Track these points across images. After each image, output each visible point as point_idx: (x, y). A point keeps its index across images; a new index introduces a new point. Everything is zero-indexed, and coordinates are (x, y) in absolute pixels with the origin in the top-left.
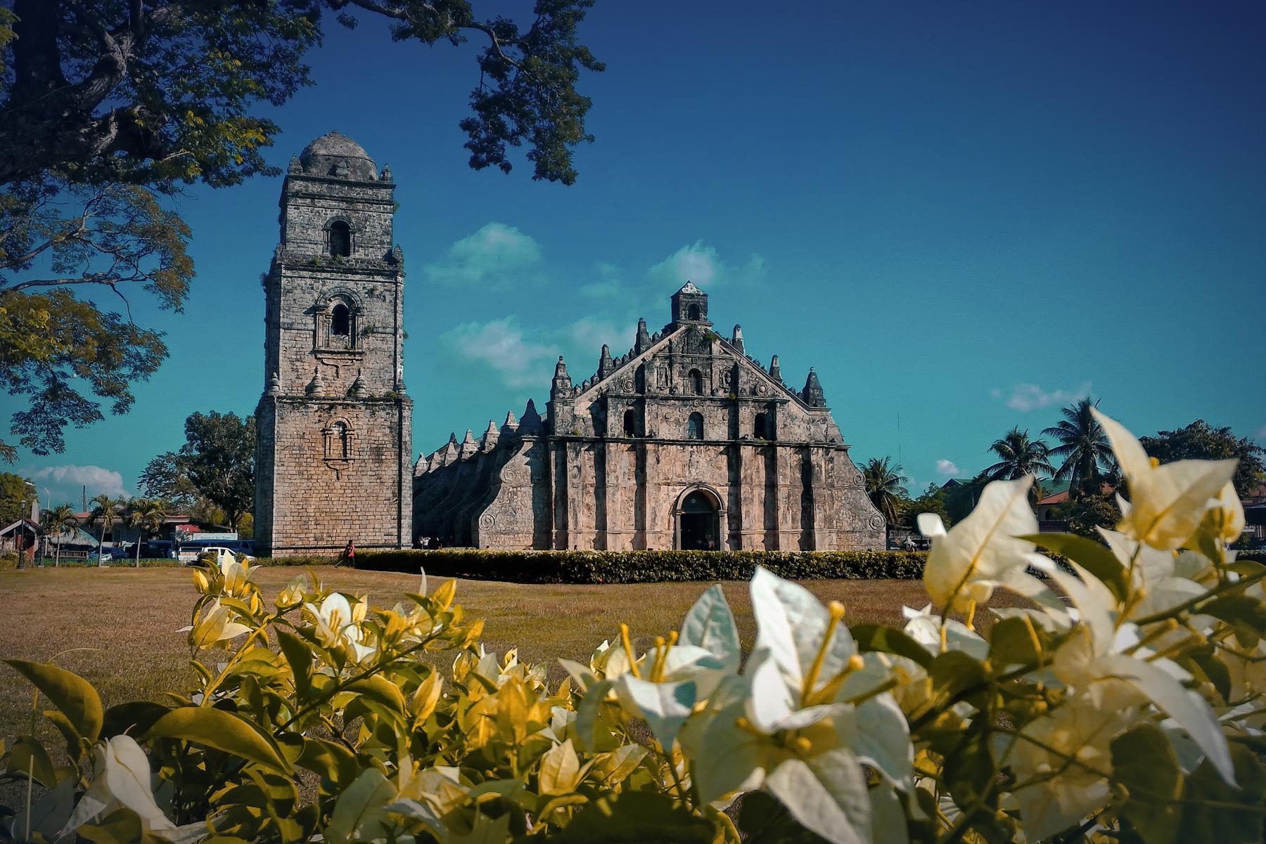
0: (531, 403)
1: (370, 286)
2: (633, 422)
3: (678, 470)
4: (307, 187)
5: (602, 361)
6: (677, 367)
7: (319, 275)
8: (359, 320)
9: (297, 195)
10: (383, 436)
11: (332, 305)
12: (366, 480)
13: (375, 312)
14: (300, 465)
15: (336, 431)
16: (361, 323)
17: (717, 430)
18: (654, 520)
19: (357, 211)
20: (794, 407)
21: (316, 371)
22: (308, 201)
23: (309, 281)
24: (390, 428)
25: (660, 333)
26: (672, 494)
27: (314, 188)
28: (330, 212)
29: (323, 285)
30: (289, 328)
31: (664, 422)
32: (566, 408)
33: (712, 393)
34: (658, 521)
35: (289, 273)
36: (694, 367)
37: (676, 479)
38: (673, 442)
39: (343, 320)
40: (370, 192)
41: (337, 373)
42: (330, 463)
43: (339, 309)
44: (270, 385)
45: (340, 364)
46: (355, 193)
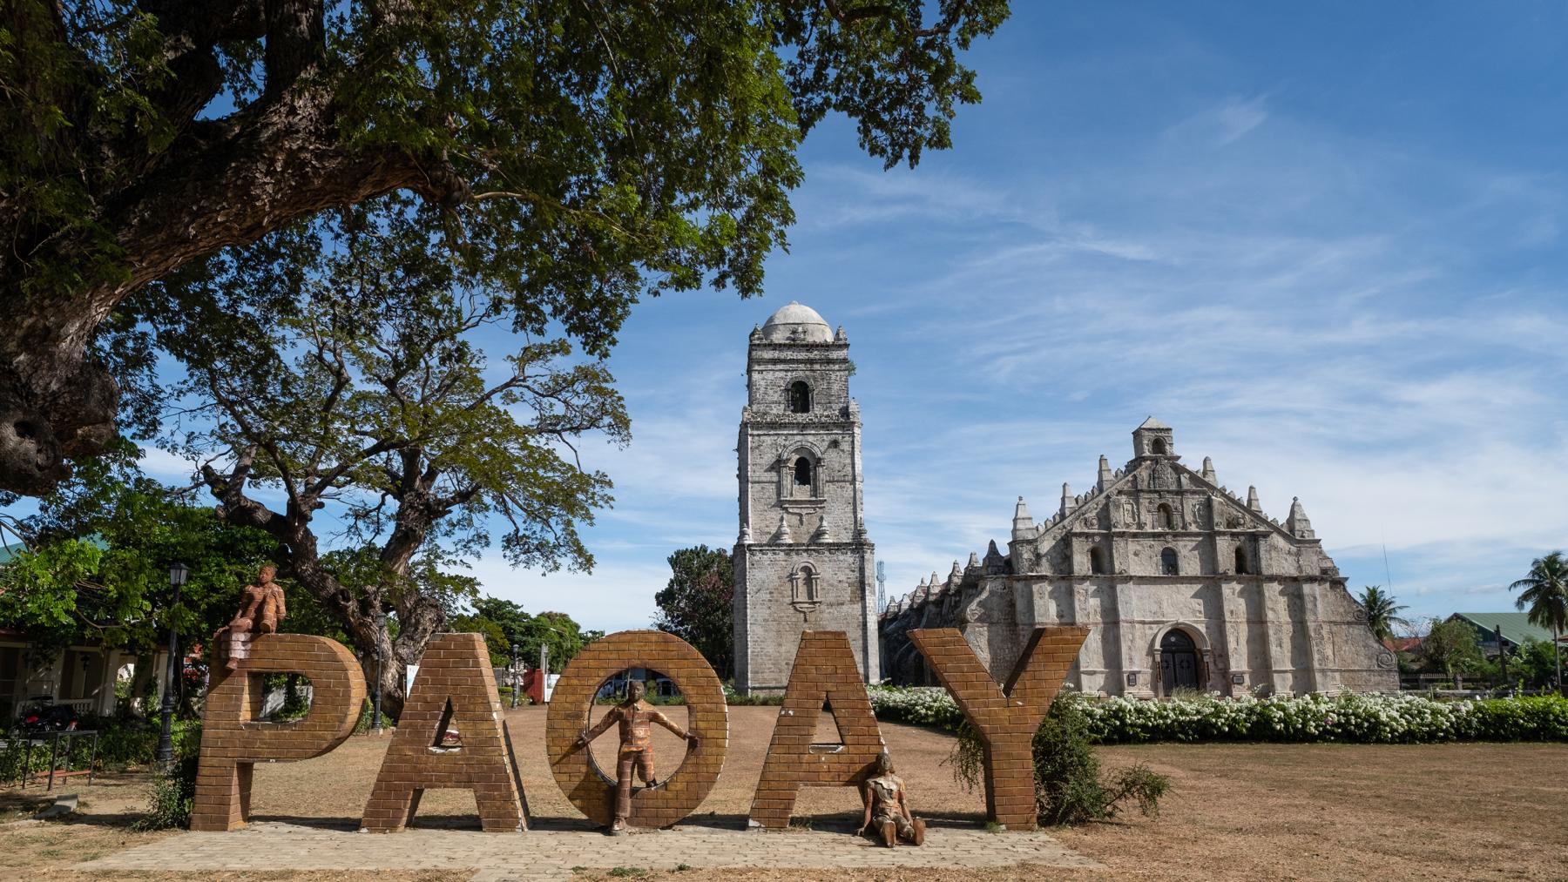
0: (992, 543)
2: (1100, 560)
5: (1063, 499)
6: (1144, 502)
8: (820, 470)
9: (760, 361)
15: (801, 575)
16: (822, 474)
17: (1190, 564)
26: (1149, 632)
31: (1135, 559)
33: (1184, 527)
39: (805, 470)
41: (801, 521)
43: (799, 462)
44: (742, 534)
45: (804, 512)
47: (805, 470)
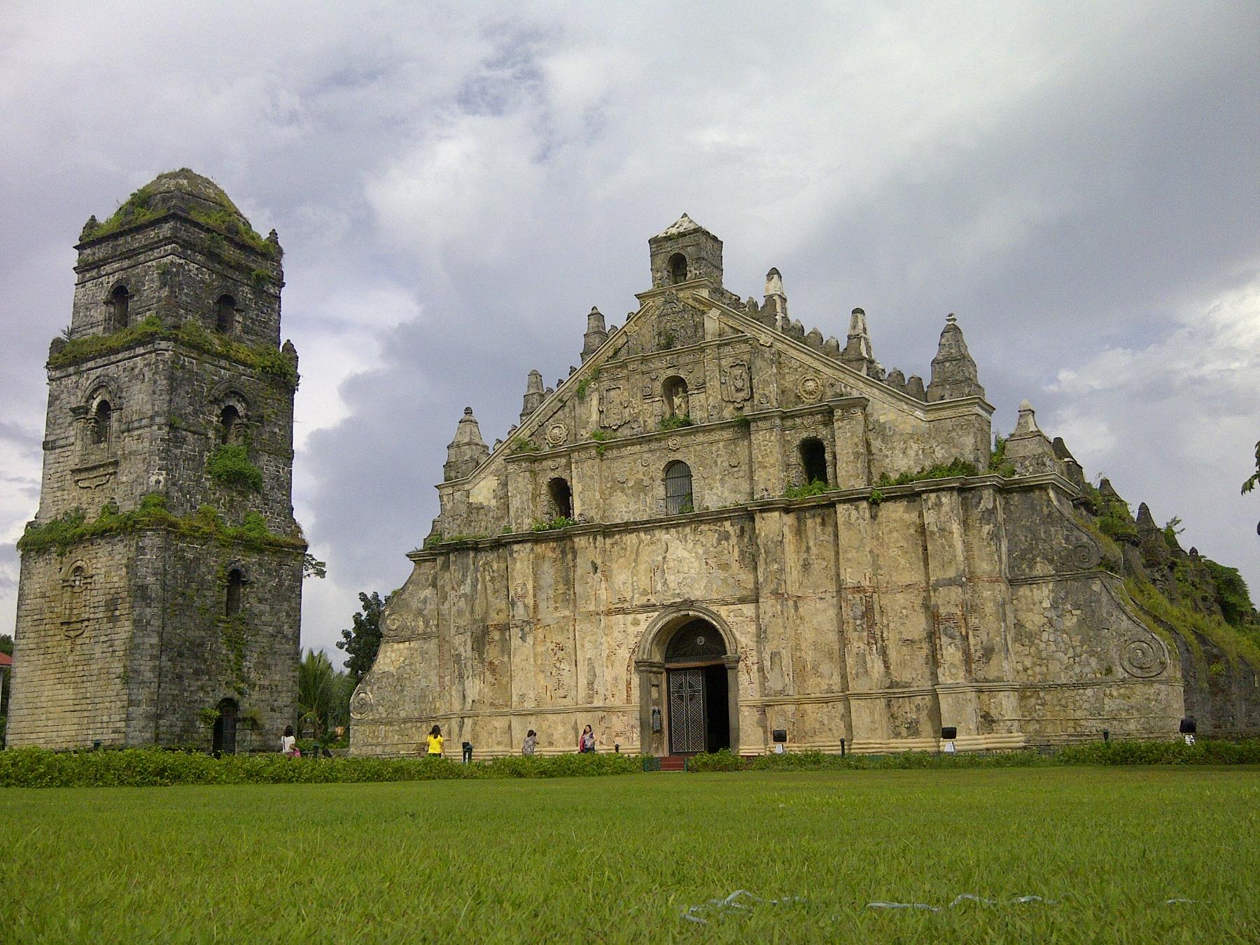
1: (131, 364)
3: (644, 582)
7: (85, 367)
8: (115, 416)
10: (119, 579)
11: (95, 403)
18: (591, 684)
20: (886, 410)
21: (74, 498)
22: (94, 273)
23: (74, 378)
24: (127, 567)
26: (632, 630)
27: (101, 252)
32: (457, 495)
35: (58, 374)
36: (671, 373)
37: (639, 600)
40: (152, 234)
42: (65, 628)
43: (104, 406)
46: (139, 240)
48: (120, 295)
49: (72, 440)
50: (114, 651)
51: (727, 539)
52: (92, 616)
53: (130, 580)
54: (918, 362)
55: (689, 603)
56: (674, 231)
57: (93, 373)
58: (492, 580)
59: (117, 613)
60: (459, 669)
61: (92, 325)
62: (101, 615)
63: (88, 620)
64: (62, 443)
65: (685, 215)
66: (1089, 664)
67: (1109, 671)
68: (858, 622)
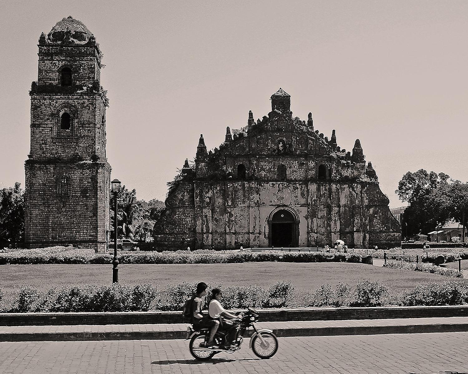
0: (186, 162)
4: (49, 50)
11: (61, 114)
12: (79, 208)
13: (86, 116)
14: (44, 199)
18: (254, 227)
19: (76, 61)
25: (261, 120)
28: (59, 62)
29: (56, 103)
30: (39, 126)
34: (257, 227)
38: (267, 182)
43: (65, 115)
47: (66, 121)
48: (66, 72)
49: (51, 126)
50: (87, 208)
51: (298, 188)
52: (74, 195)
53: (93, 183)
54: (349, 148)
55: (285, 206)
56: (280, 94)
57: (59, 100)
58: (216, 193)
59: (88, 195)
60: (207, 220)
61: (51, 79)
62: (79, 195)
63: (73, 196)
64: (44, 126)
65: (280, 88)
66: (384, 228)
67: (389, 230)
68: (335, 215)
